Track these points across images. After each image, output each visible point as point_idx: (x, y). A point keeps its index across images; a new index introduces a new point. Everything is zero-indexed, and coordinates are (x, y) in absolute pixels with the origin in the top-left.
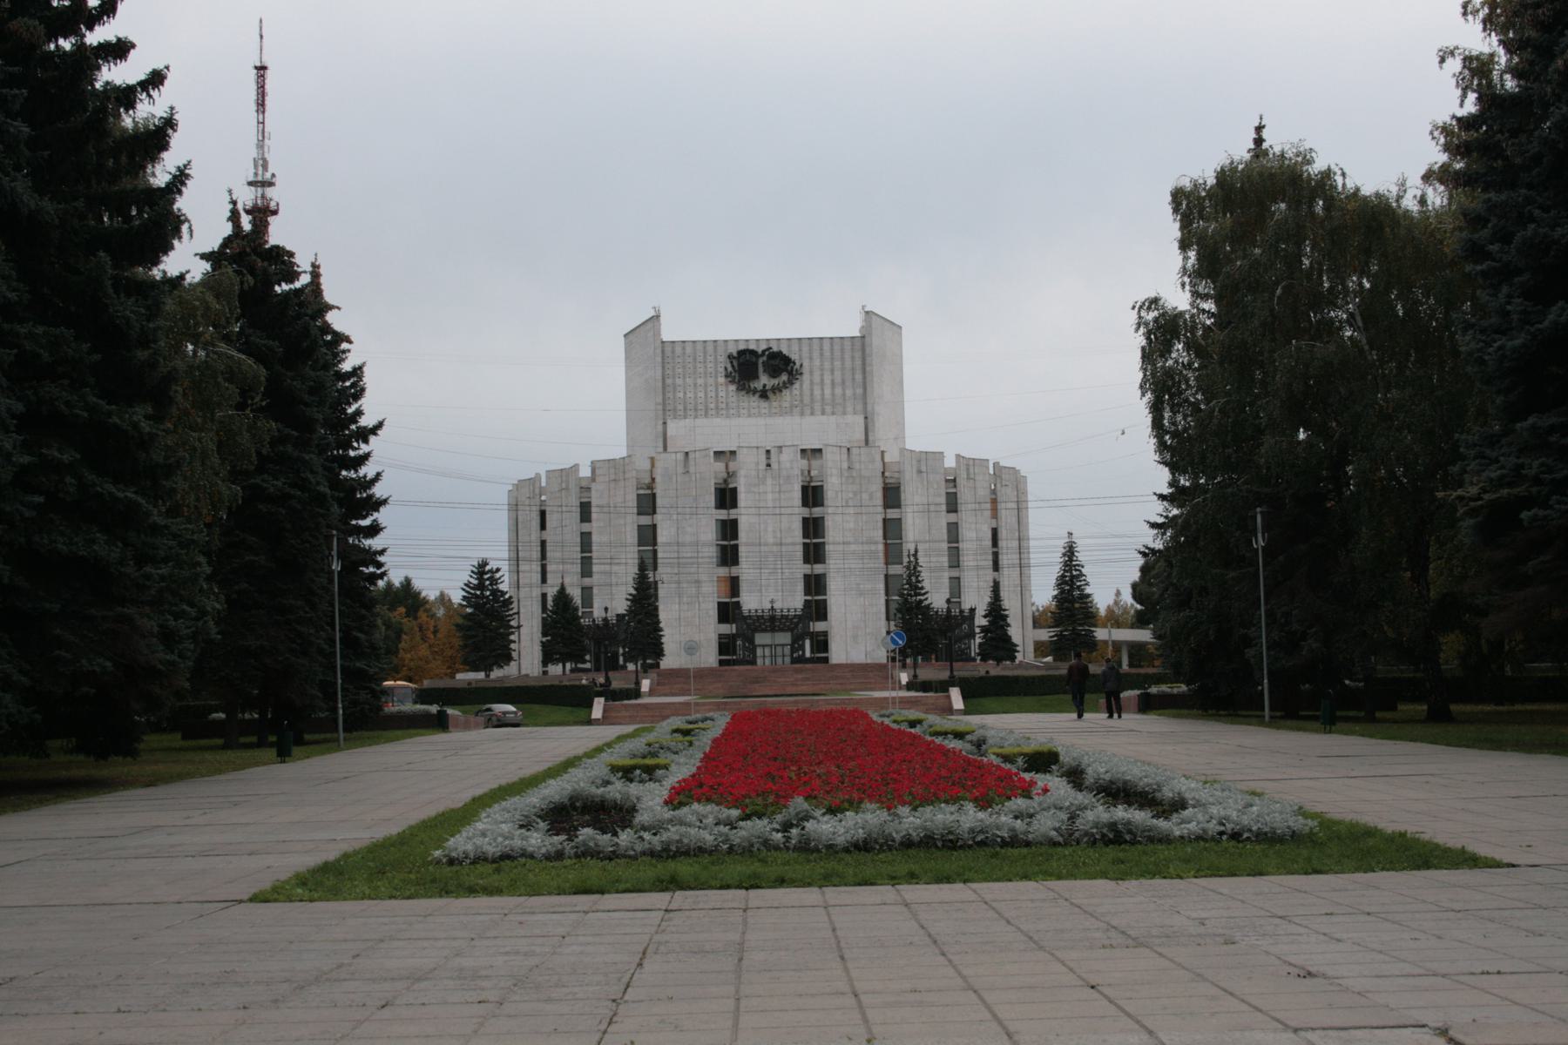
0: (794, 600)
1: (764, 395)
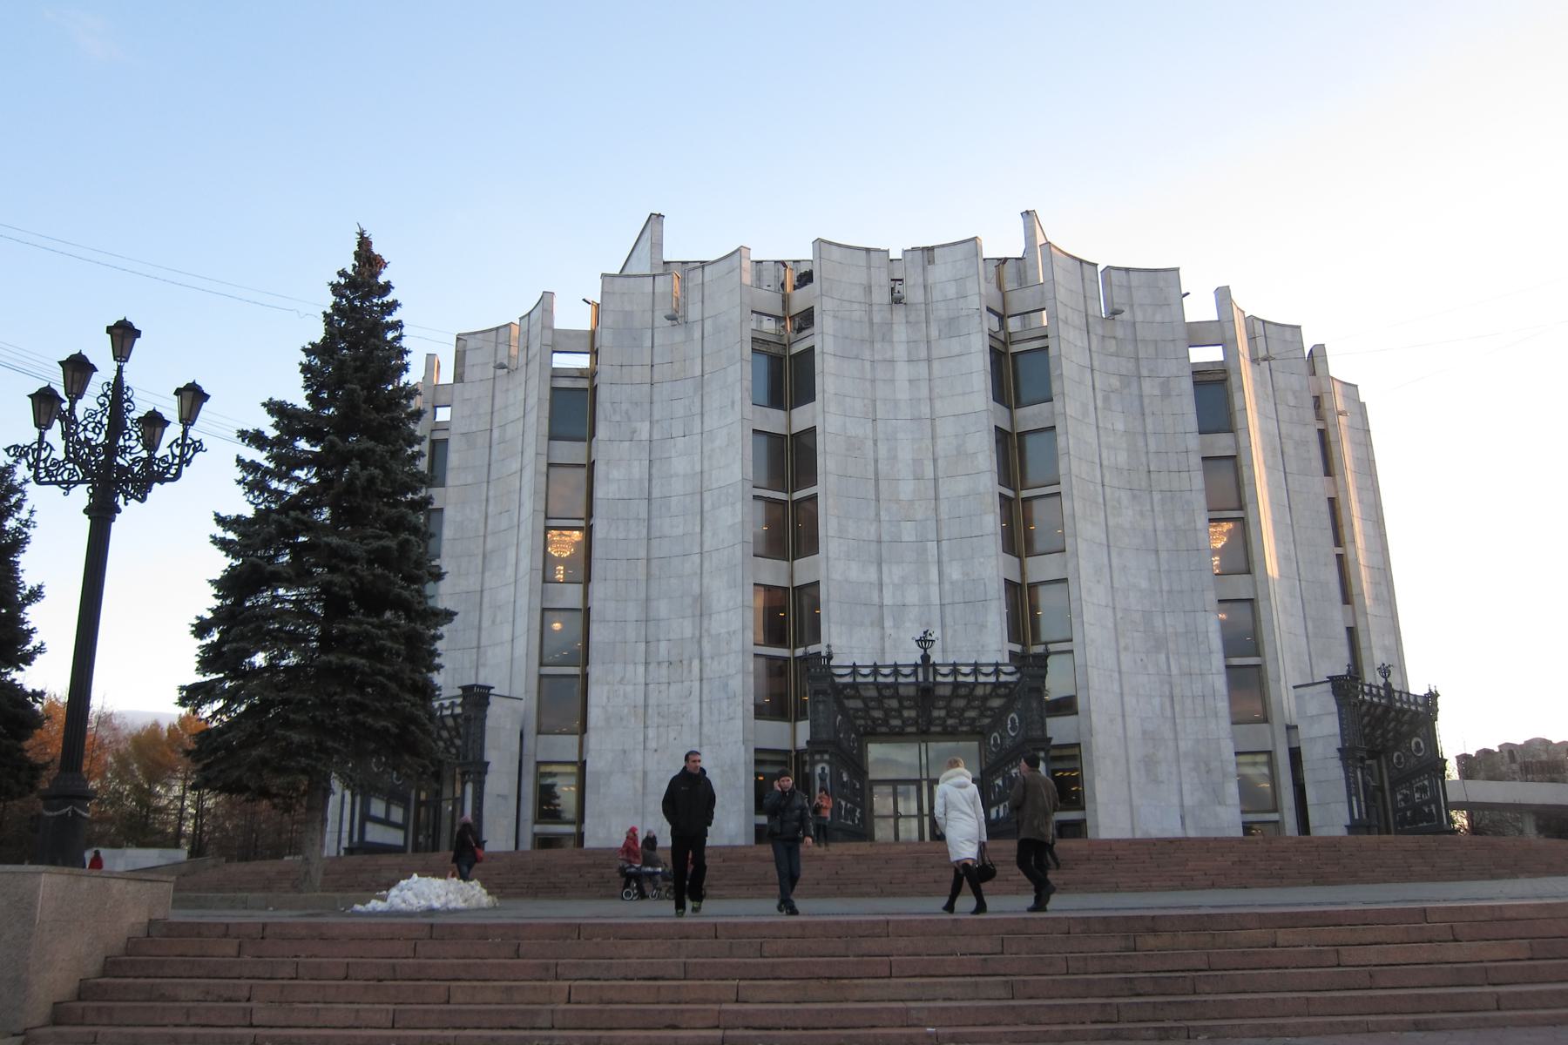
0: (983, 643)
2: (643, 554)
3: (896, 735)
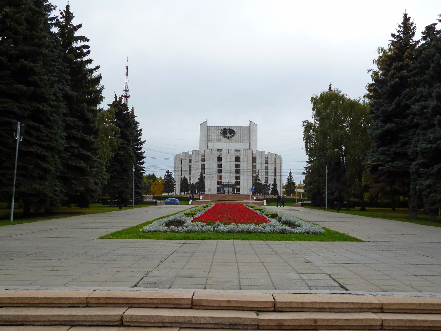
0: (233, 181)
1: (228, 138)
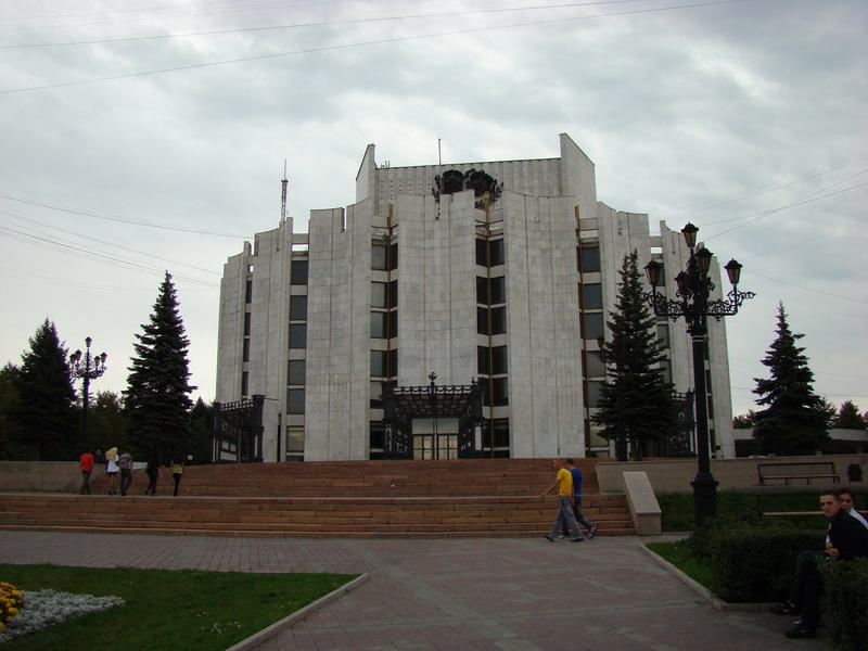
0: (461, 373)
2: (328, 336)
3: (424, 416)
